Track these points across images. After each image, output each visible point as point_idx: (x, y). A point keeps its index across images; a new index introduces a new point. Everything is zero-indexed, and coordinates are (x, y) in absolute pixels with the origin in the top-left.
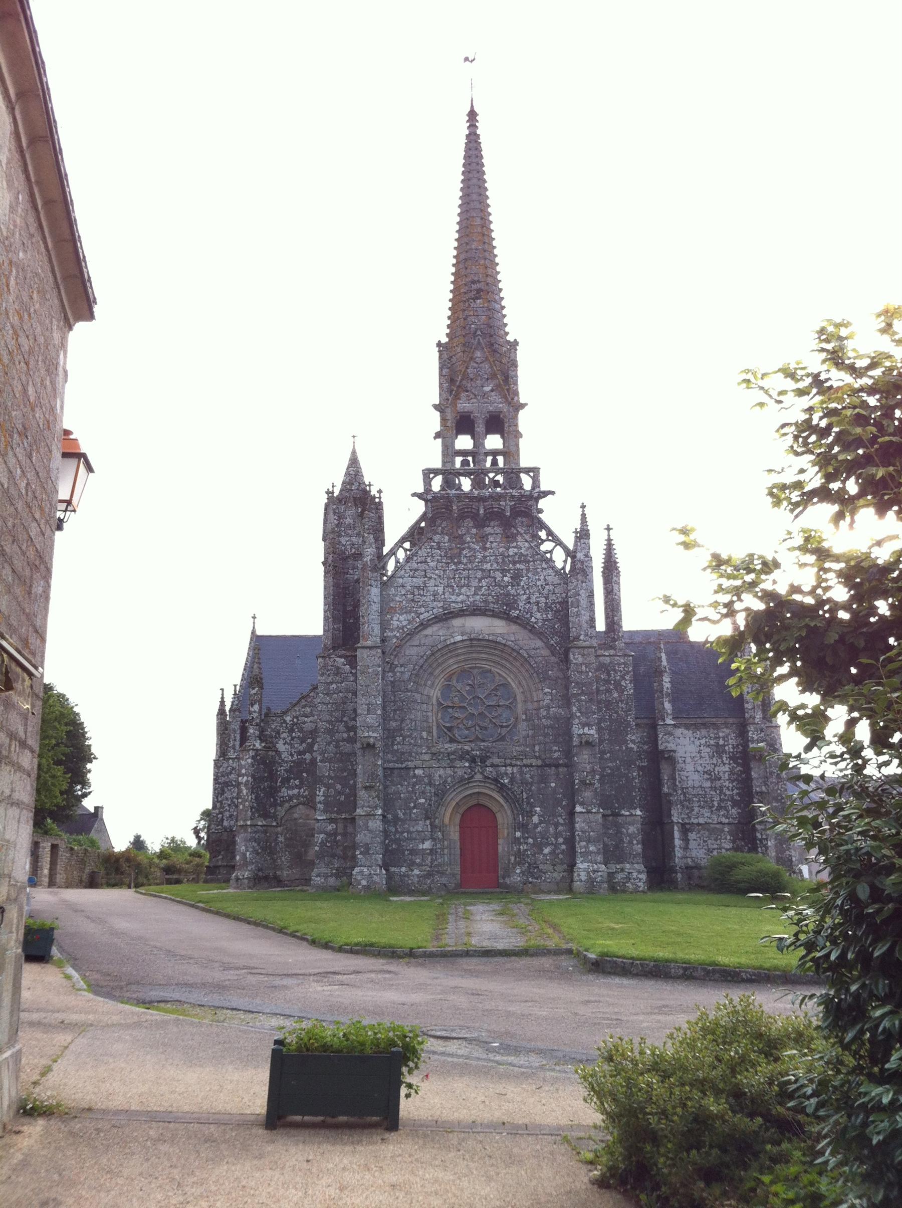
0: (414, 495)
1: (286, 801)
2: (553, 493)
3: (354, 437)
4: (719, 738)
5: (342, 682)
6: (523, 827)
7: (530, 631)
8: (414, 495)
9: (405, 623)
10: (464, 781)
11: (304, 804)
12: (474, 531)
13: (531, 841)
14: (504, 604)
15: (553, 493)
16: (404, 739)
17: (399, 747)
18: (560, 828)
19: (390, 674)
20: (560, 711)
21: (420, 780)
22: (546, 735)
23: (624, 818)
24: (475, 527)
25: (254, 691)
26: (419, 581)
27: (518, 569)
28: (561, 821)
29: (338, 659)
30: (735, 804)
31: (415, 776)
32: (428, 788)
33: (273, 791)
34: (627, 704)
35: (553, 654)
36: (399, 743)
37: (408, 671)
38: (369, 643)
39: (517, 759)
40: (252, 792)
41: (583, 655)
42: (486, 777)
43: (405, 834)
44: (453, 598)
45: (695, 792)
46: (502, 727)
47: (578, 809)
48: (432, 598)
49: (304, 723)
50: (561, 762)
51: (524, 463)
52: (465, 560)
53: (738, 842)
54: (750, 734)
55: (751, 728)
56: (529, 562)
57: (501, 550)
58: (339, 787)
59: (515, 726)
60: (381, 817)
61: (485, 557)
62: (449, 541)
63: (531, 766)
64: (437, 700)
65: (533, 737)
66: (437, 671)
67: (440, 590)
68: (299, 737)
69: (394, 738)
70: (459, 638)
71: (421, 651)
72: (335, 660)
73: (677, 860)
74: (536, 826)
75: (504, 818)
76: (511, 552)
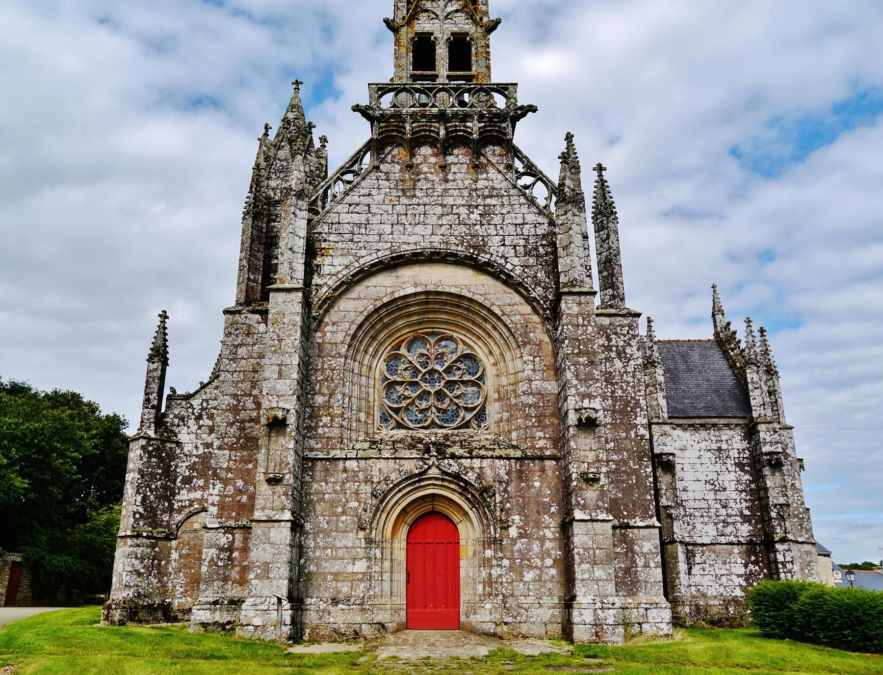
0: (357, 108)
1: (185, 507)
2: (533, 109)
3: (297, 83)
4: (721, 441)
5: (255, 344)
6: (496, 542)
7: (505, 283)
8: (357, 108)
9: (339, 268)
10: (417, 479)
12: (433, 160)
13: (506, 562)
14: (470, 246)
15: (533, 109)
16: (332, 420)
17: (326, 430)
18: (548, 545)
19: (319, 334)
20: (546, 385)
21: (353, 477)
22: (528, 417)
23: (636, 531)
24: (435, 155)
25: (155, 366)
26: (362, 218)
27: (489, 205)
28: (549, 535)
29: (250, 315)
30: (746, 519)
31: (345, 470)
32: (363, 486)
33: (168, 494)
34: (634, 377)
35: (535, 311)
36: (325, 425)
37: (342, 331)
38: (286, 285)
39: (487, 449)
40: (138, 492)
41: (580, 304)
42: (444, 473)
43: (329, 551)
44: (405, 238)
45: (697, 504)
46: (467, 409)
47: (578, 514)
48: (377, 238)
50: (548, 453)
51: (497, 78)
52: (418, 193)
53: (751, 566)
54: (762, 435)
55: (762, 427)
56: (502, 196)
57: (467, 182)
58: (240, 483)
59: (483, 408)
60: (289, 524)
61: (446, 190)
62: (401, 171)
63: (508, 458)
64: (381, 373)
65: (508, 420)
66: (382, 335)
67: (388, 229)
69: (318, 417)
70: (411, 290)
71: (361, 305)
72: (246, 317)
73: (683, 589)
74: (514, 541)
75: (469, 532)
76: (481, 184)
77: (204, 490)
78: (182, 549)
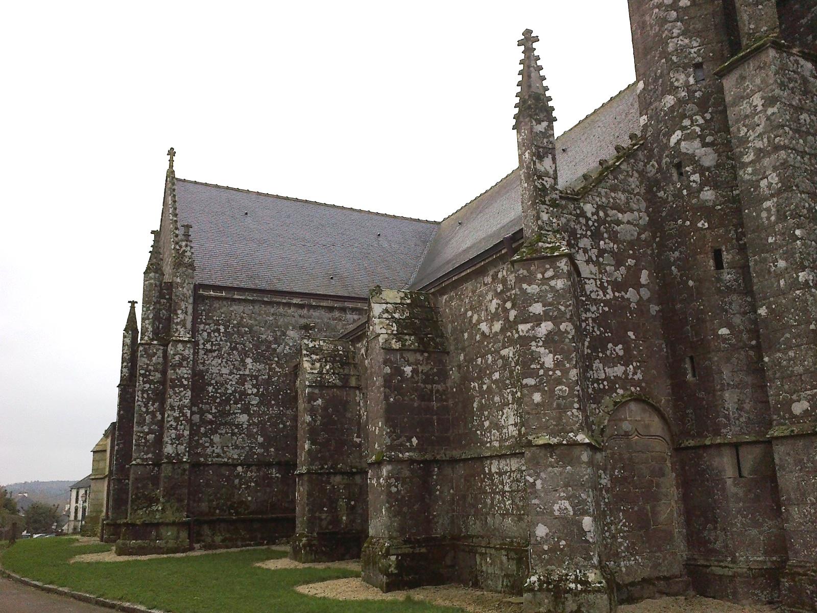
11: (637, 399)
49: (618, 222)
68: (612, 252)
77: (626, 365)
78: (614, 469)
